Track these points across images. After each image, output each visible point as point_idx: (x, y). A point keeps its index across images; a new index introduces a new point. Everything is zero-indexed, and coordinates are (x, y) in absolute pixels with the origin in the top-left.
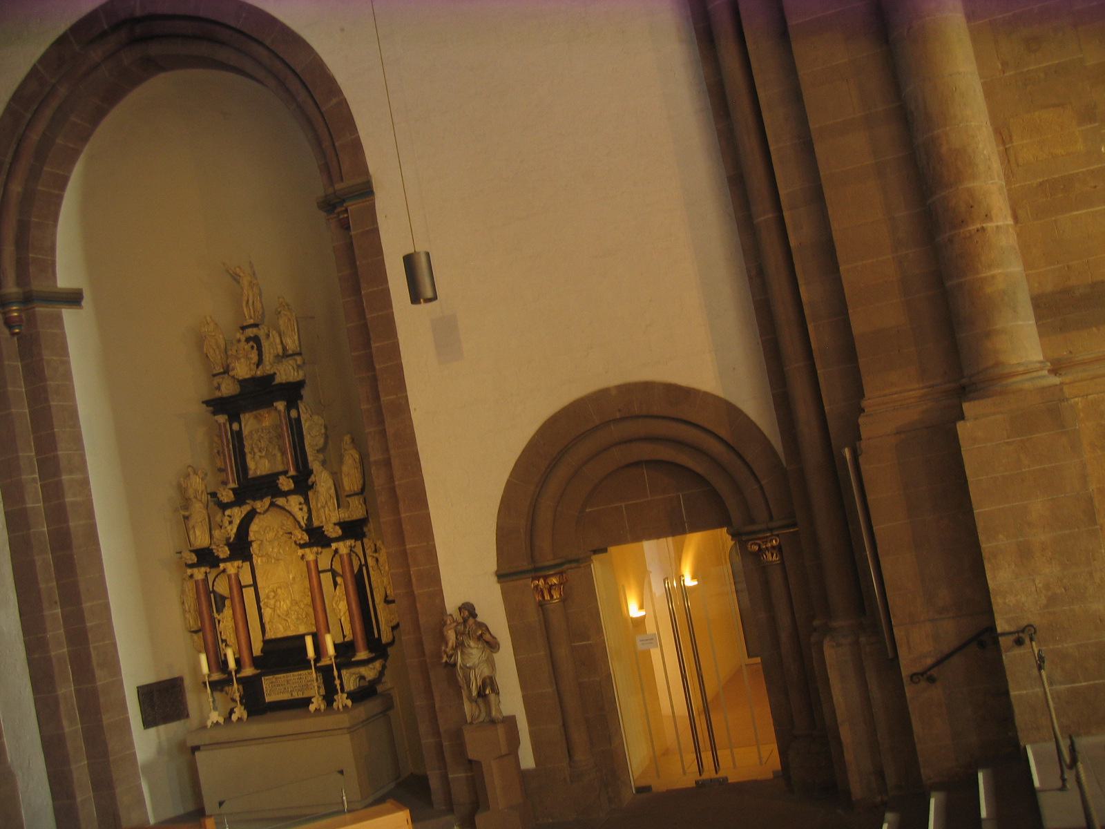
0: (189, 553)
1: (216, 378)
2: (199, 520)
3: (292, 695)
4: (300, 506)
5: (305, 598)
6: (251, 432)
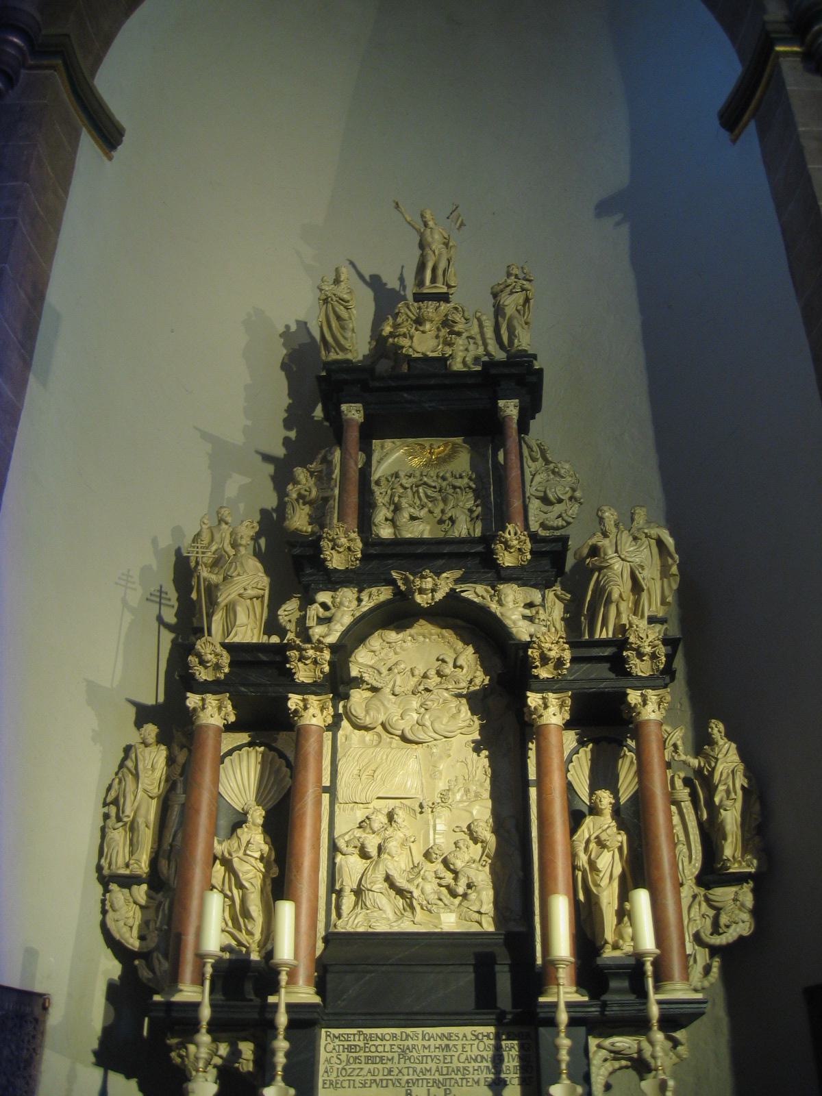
0: (219, 649)
2: (250, 592)
4: (527, 612)
6: (396, 475)
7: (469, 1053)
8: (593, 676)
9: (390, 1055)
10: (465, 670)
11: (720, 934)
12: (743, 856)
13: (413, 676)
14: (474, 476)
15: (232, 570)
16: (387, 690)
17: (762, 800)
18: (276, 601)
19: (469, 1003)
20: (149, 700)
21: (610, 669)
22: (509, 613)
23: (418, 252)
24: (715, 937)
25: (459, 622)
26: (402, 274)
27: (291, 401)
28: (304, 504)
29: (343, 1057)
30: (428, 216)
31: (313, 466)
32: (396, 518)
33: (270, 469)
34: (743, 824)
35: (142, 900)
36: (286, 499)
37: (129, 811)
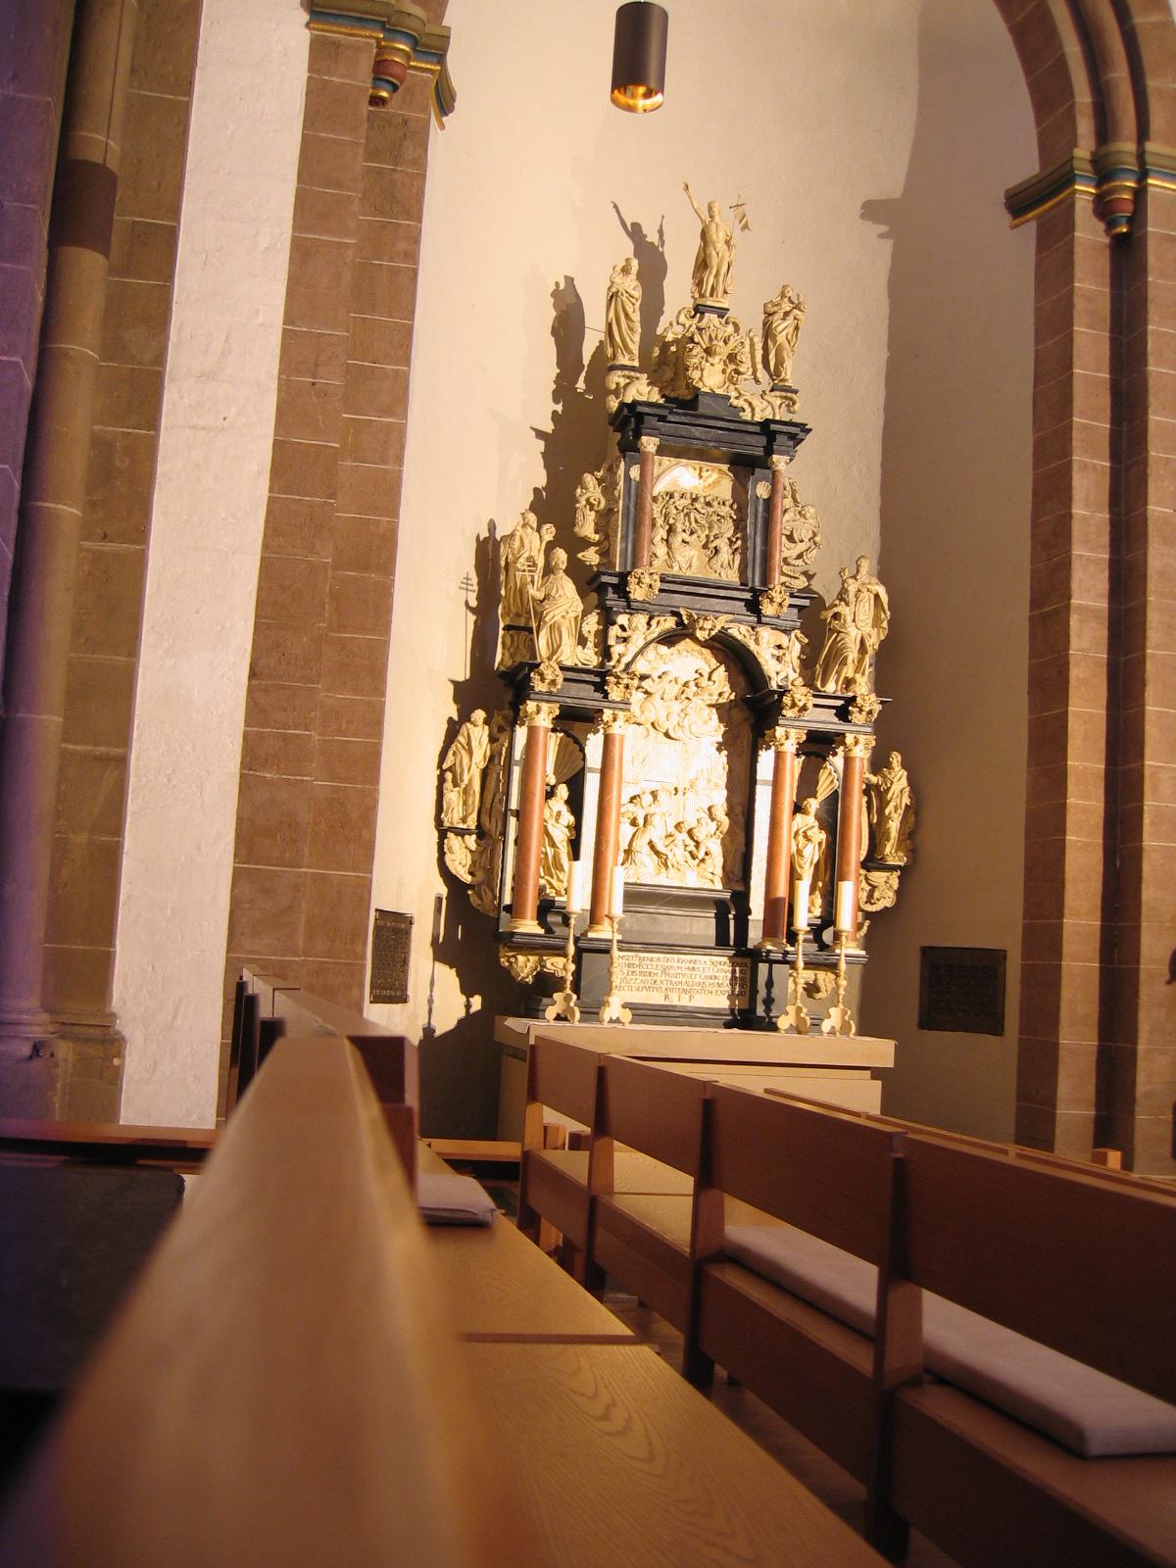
1: (619, 372)
3: (666, 997)
5: (707, 824)
7: (707, 974)
8: (822, 718)
9: (656, 972)
10: (717, 683)
11: (872, 904)
12: (896, 851)
13: (676, 682)
14: (735, 507)
15: (554, 590)
16: (657, 696)
17: (917, 814)
18: (585, 613)
19: (713, 944)
20: (461, 678)
21: (835, 714)
22: (763, 654)
23: (698, 242)
24: (868, 905)
25: (717, 645)
26: (661, 226)
27: (558, 371)
28: (591, 510)
29: (625, 971)
30: (715, 209)
31: (599, 474)
32: (670, 540)
33: (541, 445)
34: (901, 831)
35: (473, 846)
36: (578, 505)
37: (466, 778)
